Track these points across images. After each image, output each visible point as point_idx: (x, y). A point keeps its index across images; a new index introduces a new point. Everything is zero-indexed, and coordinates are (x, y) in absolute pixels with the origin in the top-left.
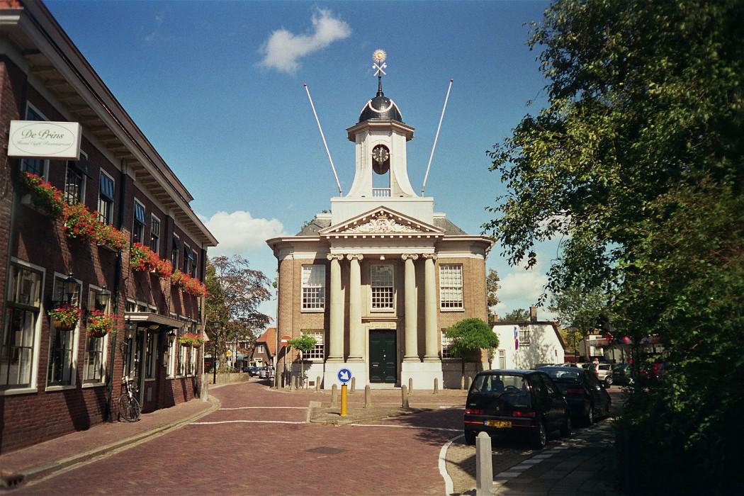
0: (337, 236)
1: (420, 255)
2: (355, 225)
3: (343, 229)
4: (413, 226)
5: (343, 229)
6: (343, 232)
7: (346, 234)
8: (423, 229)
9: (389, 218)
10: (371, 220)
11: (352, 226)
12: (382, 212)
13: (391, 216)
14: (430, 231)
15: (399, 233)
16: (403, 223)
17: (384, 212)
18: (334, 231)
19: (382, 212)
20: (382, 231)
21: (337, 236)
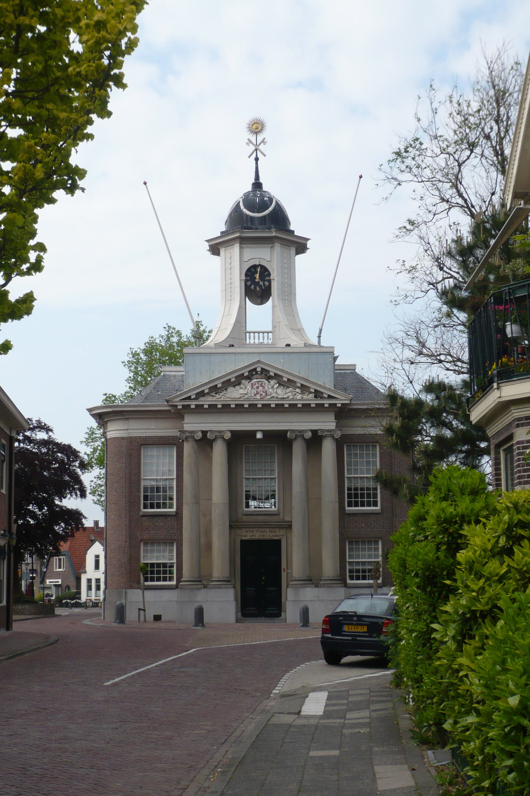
1: (314, 432)
3: (202, 394)
4: (304, 388)
5: (202, 394)
7: (206, 402)
11: (215, 389)
12: (259, 369)
13: (272, 374)
14: (330, 397)
15: (283, 399)
16: (290, 383)
17: (262, 369)
18: (189, 398)
19: (259, 369)
20: (258, 397)
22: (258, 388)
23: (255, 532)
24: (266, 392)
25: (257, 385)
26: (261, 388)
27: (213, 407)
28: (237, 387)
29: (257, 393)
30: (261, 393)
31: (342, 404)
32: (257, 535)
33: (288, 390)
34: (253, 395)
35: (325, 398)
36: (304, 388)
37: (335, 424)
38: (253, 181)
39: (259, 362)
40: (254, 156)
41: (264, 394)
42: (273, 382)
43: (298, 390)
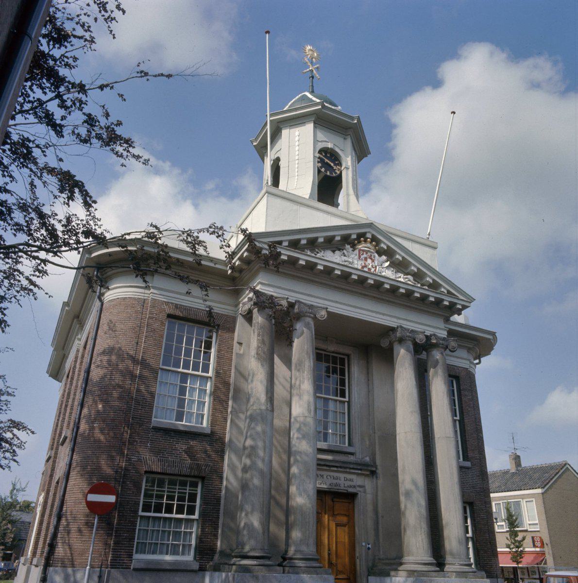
0: (285, 254)
3: (295, 245)
4: (418, 276)
9: (380, 253)
10: (348, 247)
11: (313, 244)
12: (369, 236)
16: (400, 266)
17: (373, 235)
22: (366, 259)
23: (325, 477)
24: (376, 267)
25: (365, 255)
26: (369, 261)
27: (311, 267)
28: (337, 252)
29: (366, 266)
30: (370, 267)
32: (342, 486)
36: (418, 276)
42: (384, 258)
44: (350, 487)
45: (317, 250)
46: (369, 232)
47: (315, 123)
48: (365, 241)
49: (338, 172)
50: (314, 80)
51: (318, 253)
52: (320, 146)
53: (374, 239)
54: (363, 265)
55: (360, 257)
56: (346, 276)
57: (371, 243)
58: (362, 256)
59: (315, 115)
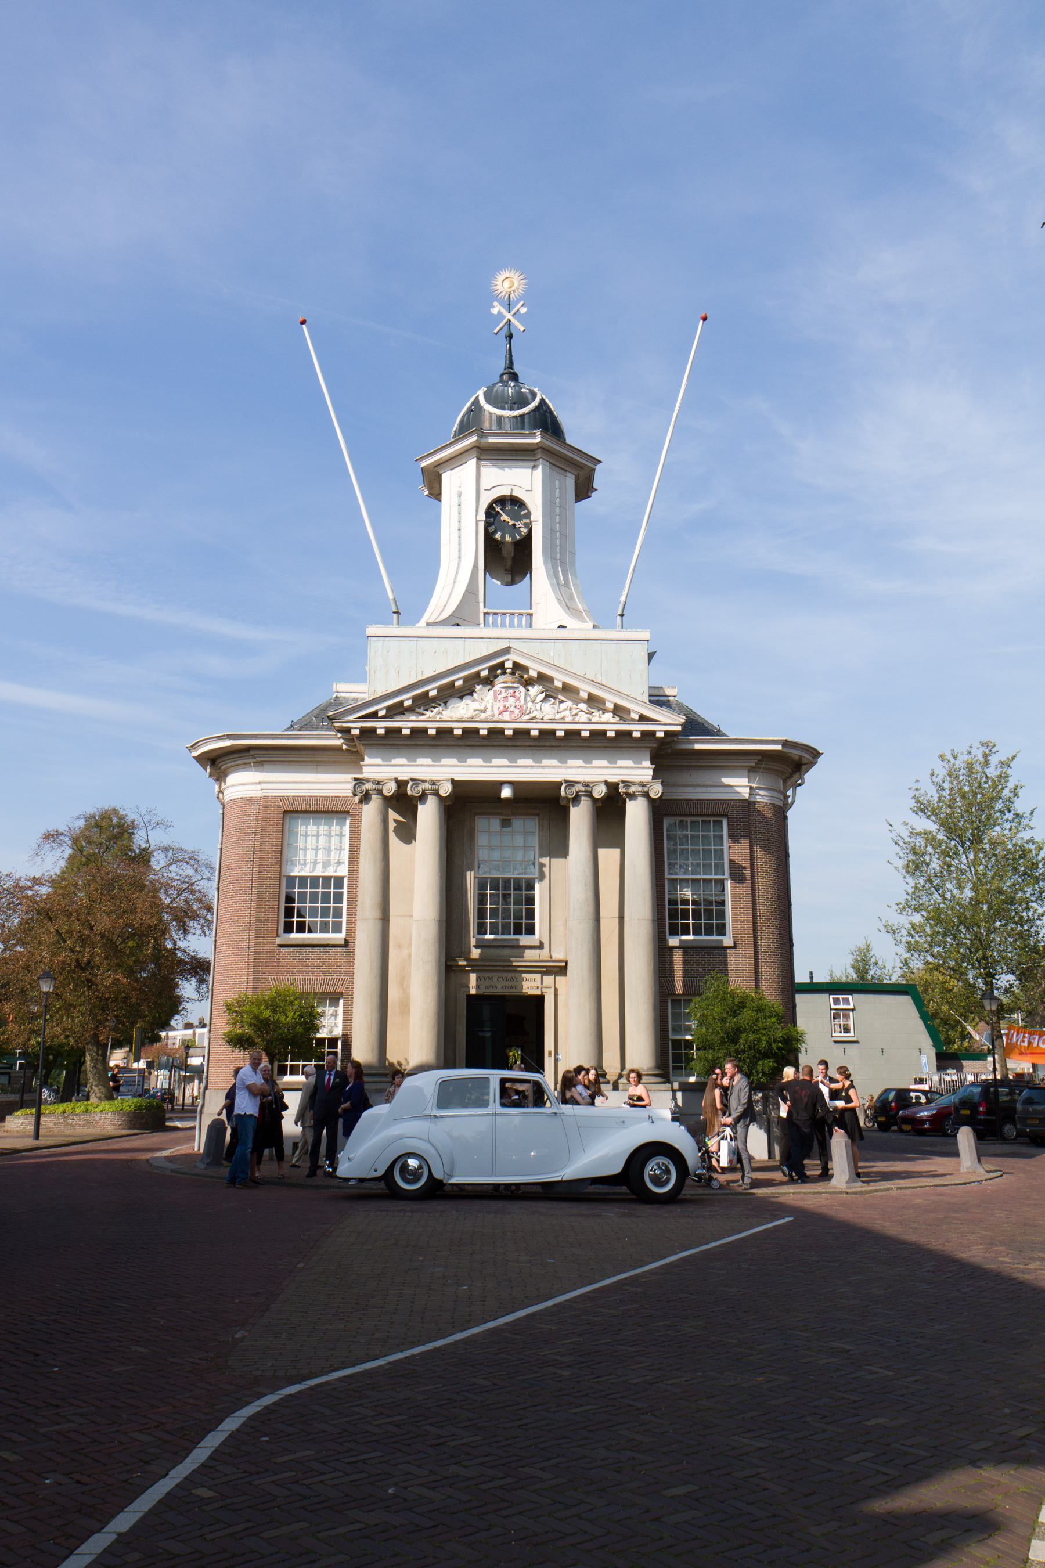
0: (381, 727)
2: (434, 699)
6: (398, 718)
7: (406, 724)
8: (617, 710)
9: (528, 683)
10: (478, 688)
11: (423, 702)
12: (509, 665)
13: (533, 674)
14: (643, 718)
15: (552, 721)
18: (374, 715)
19: (509, 665)
20: (506, 716)
21: (381, 727)
23: (495, 979)
25: (504, 695)
26: (511, 700)
30: (512, 709)
31: (666, 733)
33: (563, 706)
34: (496, 713)
35: (633, 720)
36: (593, 700)
37: (651, 772)
38: (502, 371)
39: (507, 650)
40: (505, 331)
41: (517, 712)
42: (534, 690)
43: (583, 706)
44: (532, 988)
45: (433, 705)
46: (508, 660)
47: (479, 459)
48: (504, 673)
49: (524, 531)
50: (512, 340)
51: (435, 708)
52: (487, 499)
53: (516, 666)
54: (502, 708)
55: (495, 697)
56: (470, 734)
57: (513, 673)
58: (500, 697)
59: (475, 449)
